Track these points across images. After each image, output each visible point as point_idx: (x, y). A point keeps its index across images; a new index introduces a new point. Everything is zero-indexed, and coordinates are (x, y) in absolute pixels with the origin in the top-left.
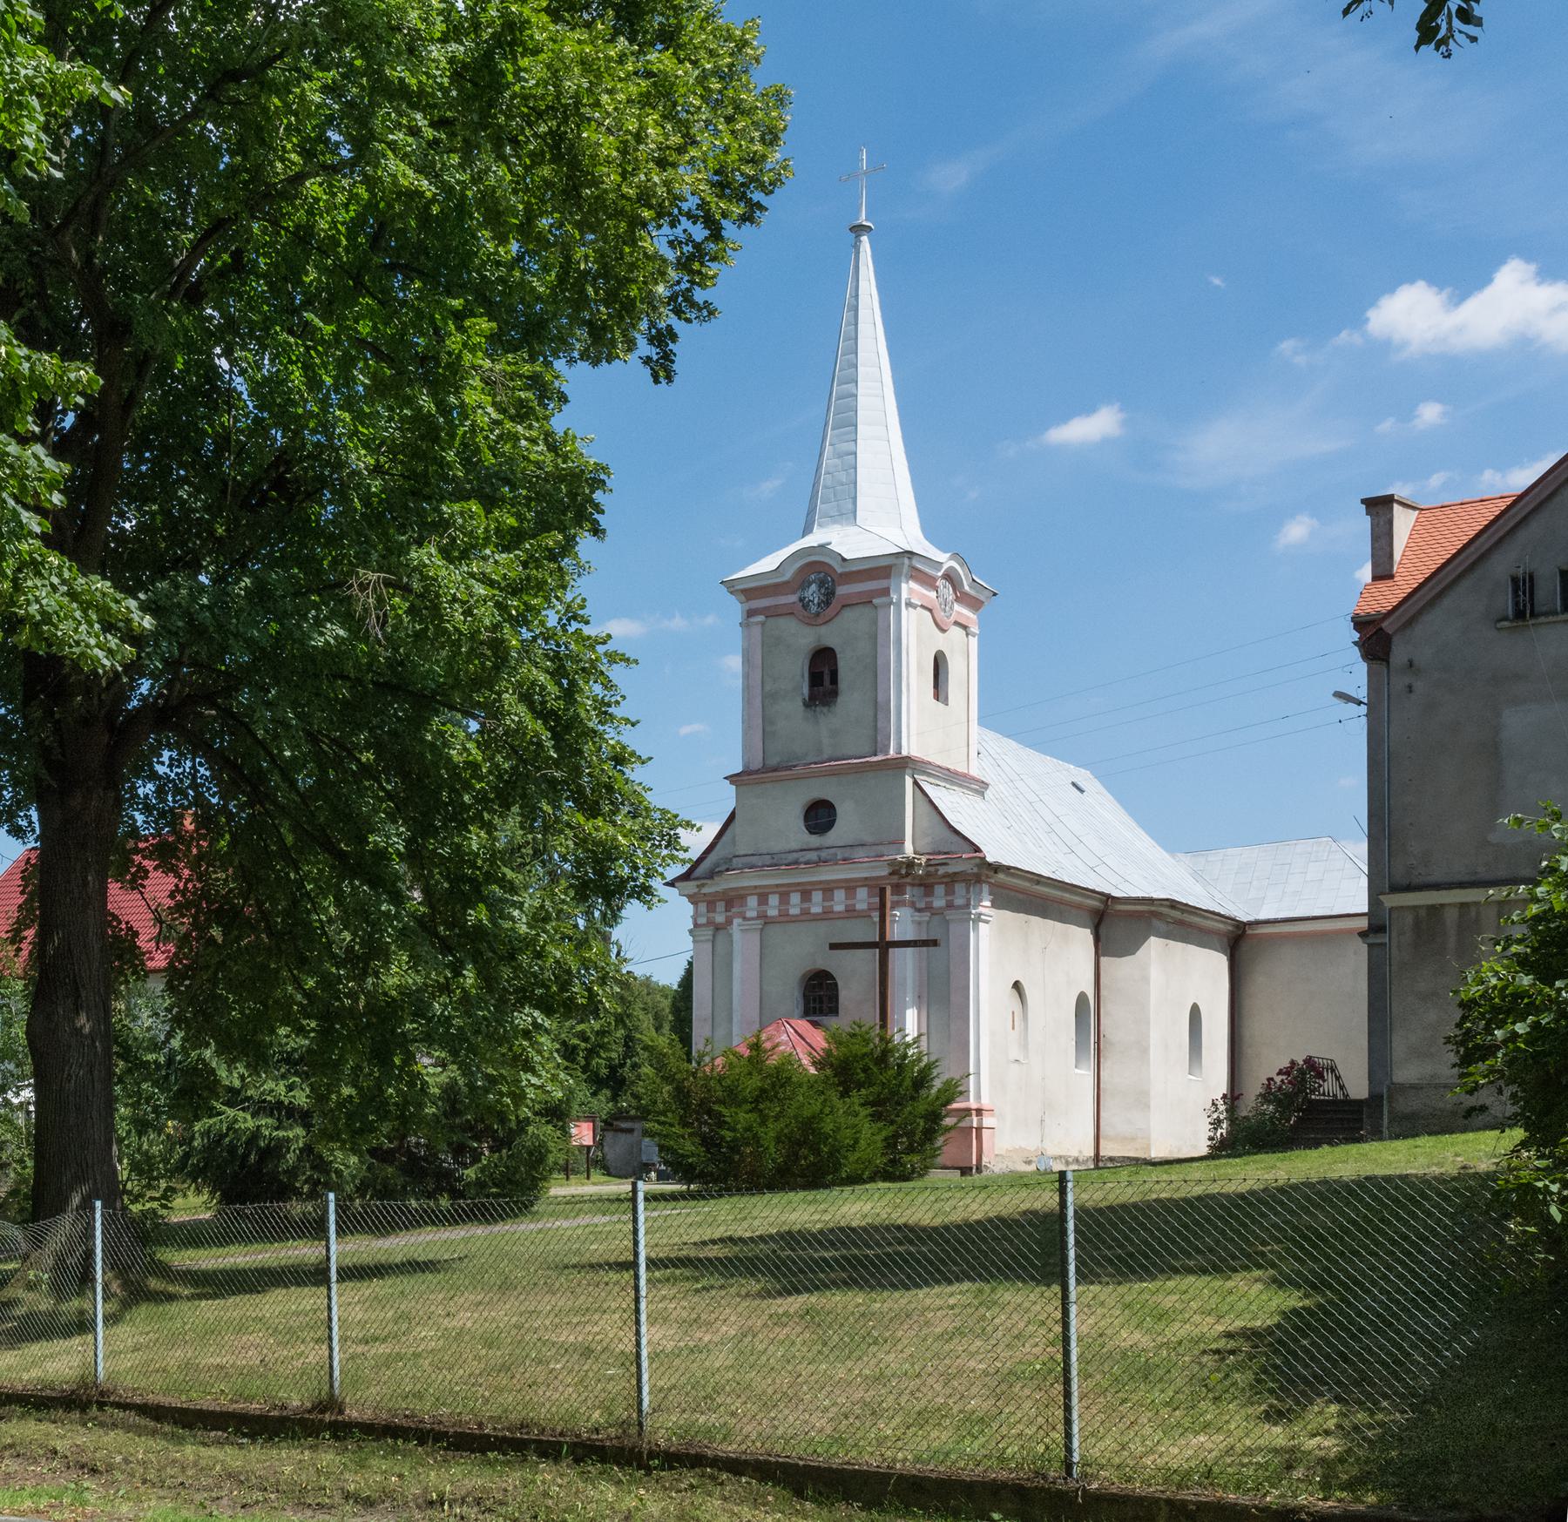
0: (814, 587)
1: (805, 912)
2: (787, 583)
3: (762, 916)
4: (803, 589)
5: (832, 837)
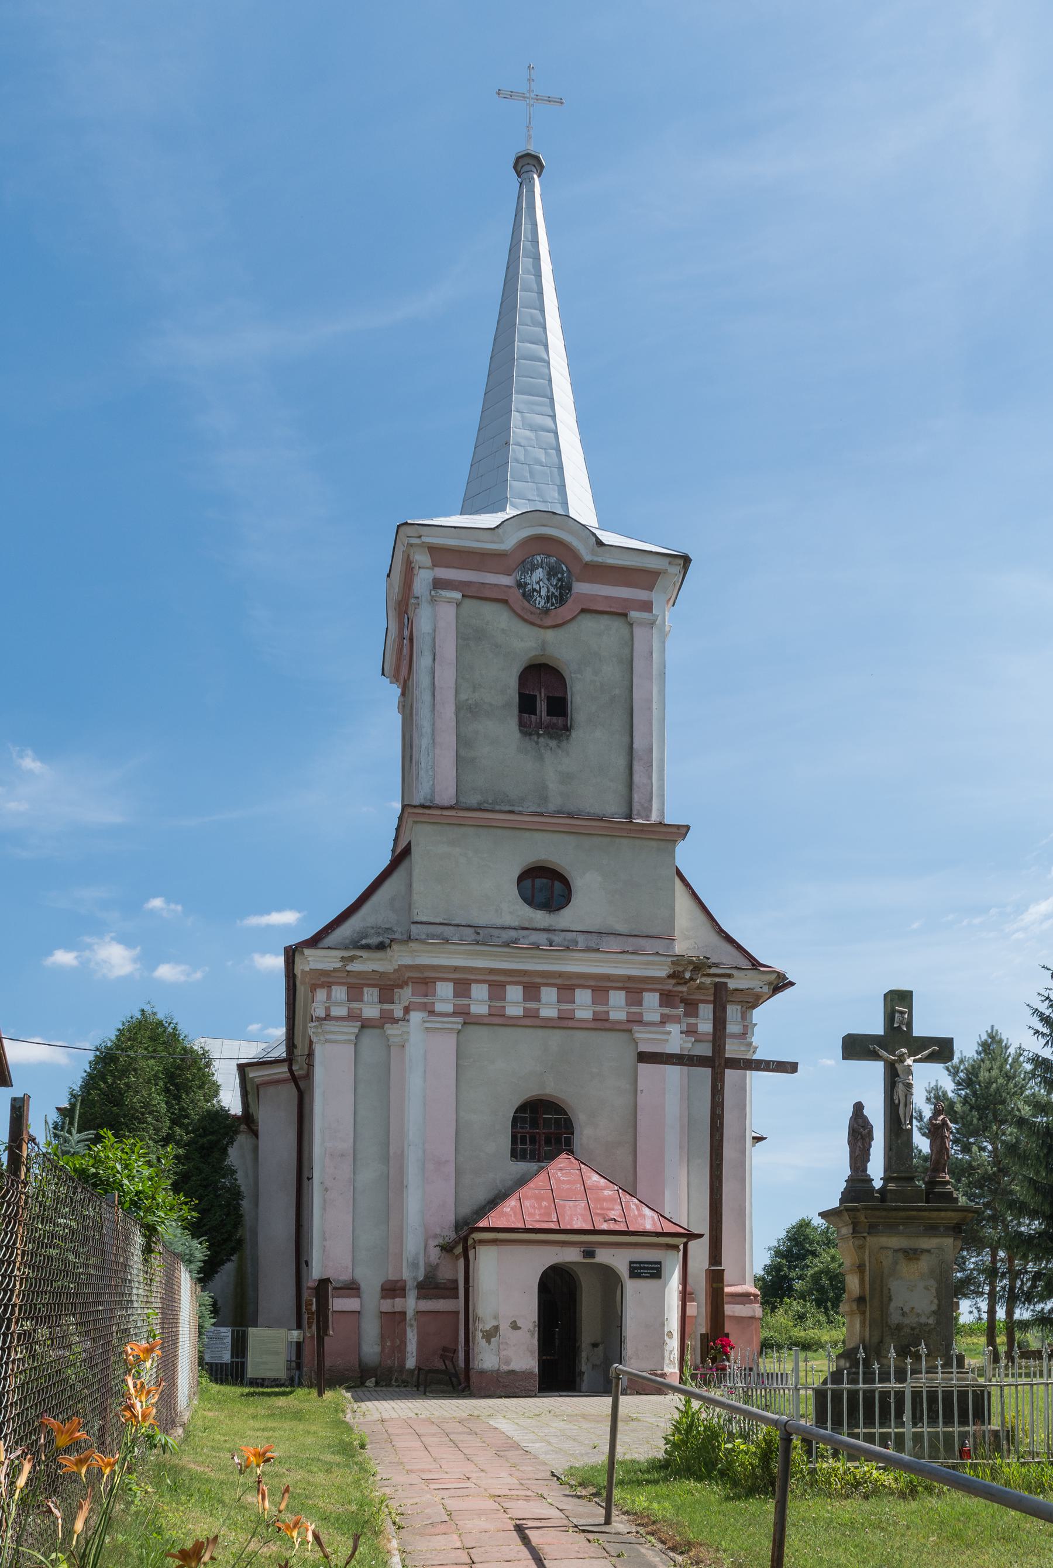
0: (539, 573)
1: (531, 1015)
2: (501, 555)
3: (462, 1012)
4: (525, 572)
5: (566, 918)
